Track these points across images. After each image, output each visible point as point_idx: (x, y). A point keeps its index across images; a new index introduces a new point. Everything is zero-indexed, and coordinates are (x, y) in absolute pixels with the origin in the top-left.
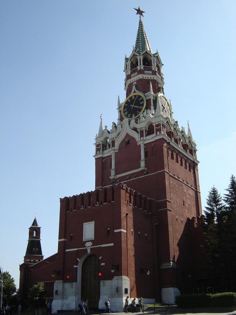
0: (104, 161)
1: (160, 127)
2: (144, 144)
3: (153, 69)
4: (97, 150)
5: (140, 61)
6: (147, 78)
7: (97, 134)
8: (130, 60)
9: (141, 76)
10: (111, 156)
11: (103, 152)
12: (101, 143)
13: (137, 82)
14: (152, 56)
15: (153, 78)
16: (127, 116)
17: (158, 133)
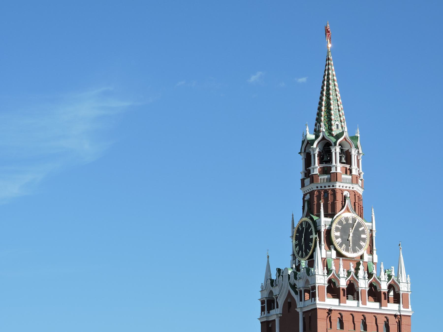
0: (270, 326)
1: (315, 292)
2: (304, 313)
3: (333, 170)
4: (263, 309)
5: (314, 155)
6: (323, 188)
7: (262, 284)
8: (305, 151)
9: (313, 187)
10: (274, 320)
11: (269, 313)
12: (265, 299)
13: (310, 196)
14: (333, 144)
15: (333, 186)
16: (298, 253)
17: (313, 299)
